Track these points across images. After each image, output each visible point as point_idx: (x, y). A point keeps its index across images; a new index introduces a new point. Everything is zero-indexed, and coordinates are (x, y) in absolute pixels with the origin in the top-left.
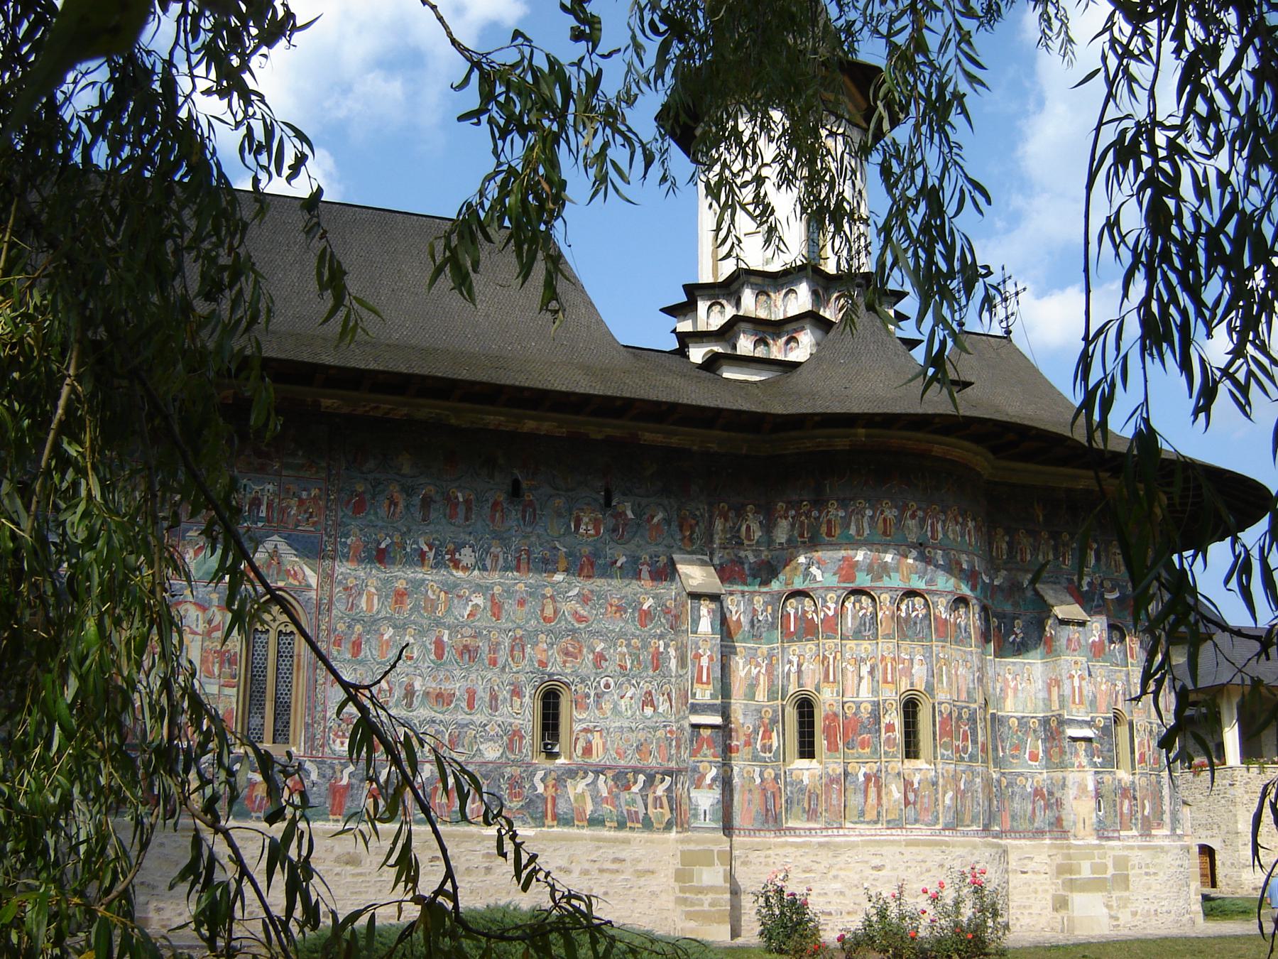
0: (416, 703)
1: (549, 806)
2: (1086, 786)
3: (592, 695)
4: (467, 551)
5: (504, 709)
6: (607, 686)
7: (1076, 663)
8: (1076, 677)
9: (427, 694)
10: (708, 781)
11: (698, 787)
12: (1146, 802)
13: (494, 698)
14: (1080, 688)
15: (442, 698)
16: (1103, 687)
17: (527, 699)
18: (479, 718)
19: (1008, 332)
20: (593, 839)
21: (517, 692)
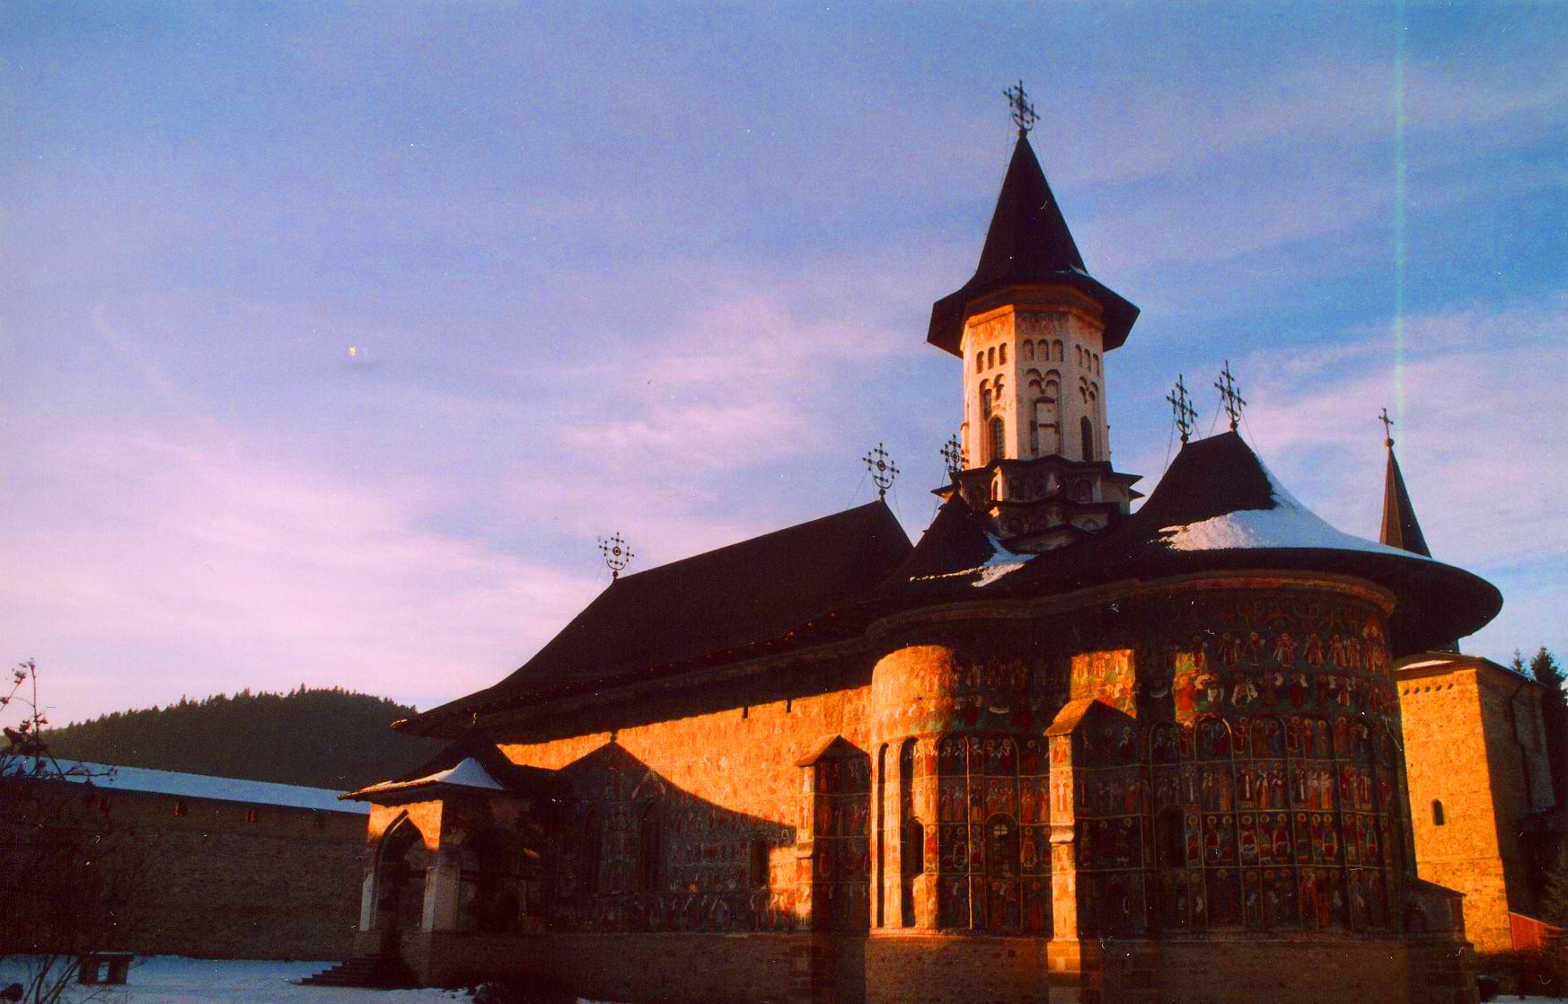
0: (702, 858)
1: (757, 917)
2: (1067, 887)
3: (777, 841)
4: (723, 759)
5: (737, 857)
6: (785, 835)
7: (1062, 773)
8: (1062, 785)
9: (705, 850)
10: (804, 897)
11: (800, 902)
12: (1200, 901)
13: (733, 849)
14: (1065, 795)
15: (711, 853)
16: (1132, 788)
17: (748, 850)
18: (727, 864)
19: (1234, 425)
20: (775, 938)
21: (743, 845)
